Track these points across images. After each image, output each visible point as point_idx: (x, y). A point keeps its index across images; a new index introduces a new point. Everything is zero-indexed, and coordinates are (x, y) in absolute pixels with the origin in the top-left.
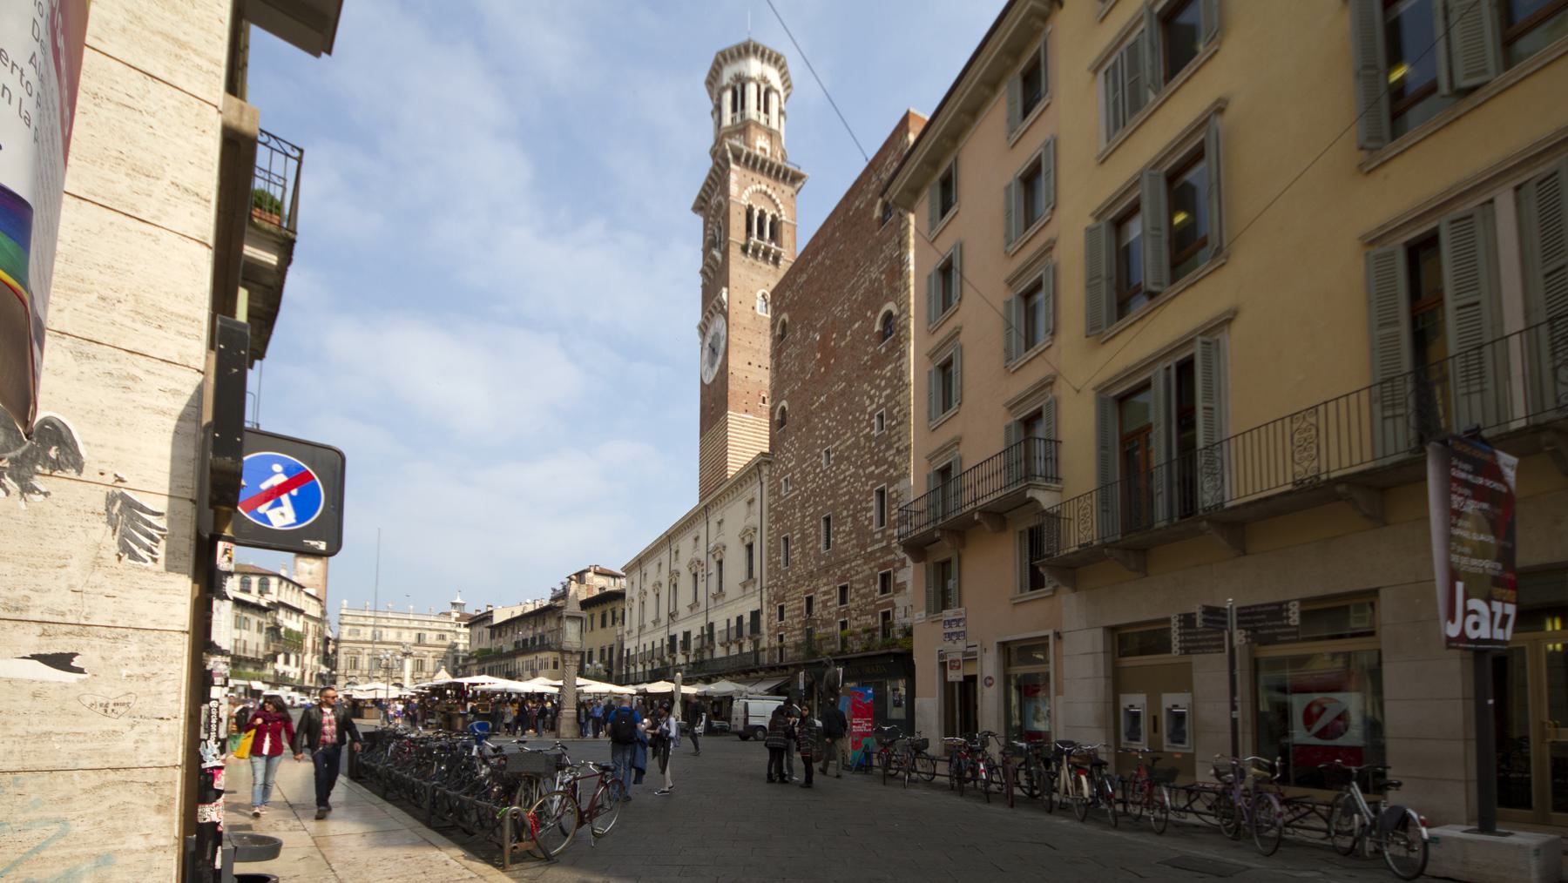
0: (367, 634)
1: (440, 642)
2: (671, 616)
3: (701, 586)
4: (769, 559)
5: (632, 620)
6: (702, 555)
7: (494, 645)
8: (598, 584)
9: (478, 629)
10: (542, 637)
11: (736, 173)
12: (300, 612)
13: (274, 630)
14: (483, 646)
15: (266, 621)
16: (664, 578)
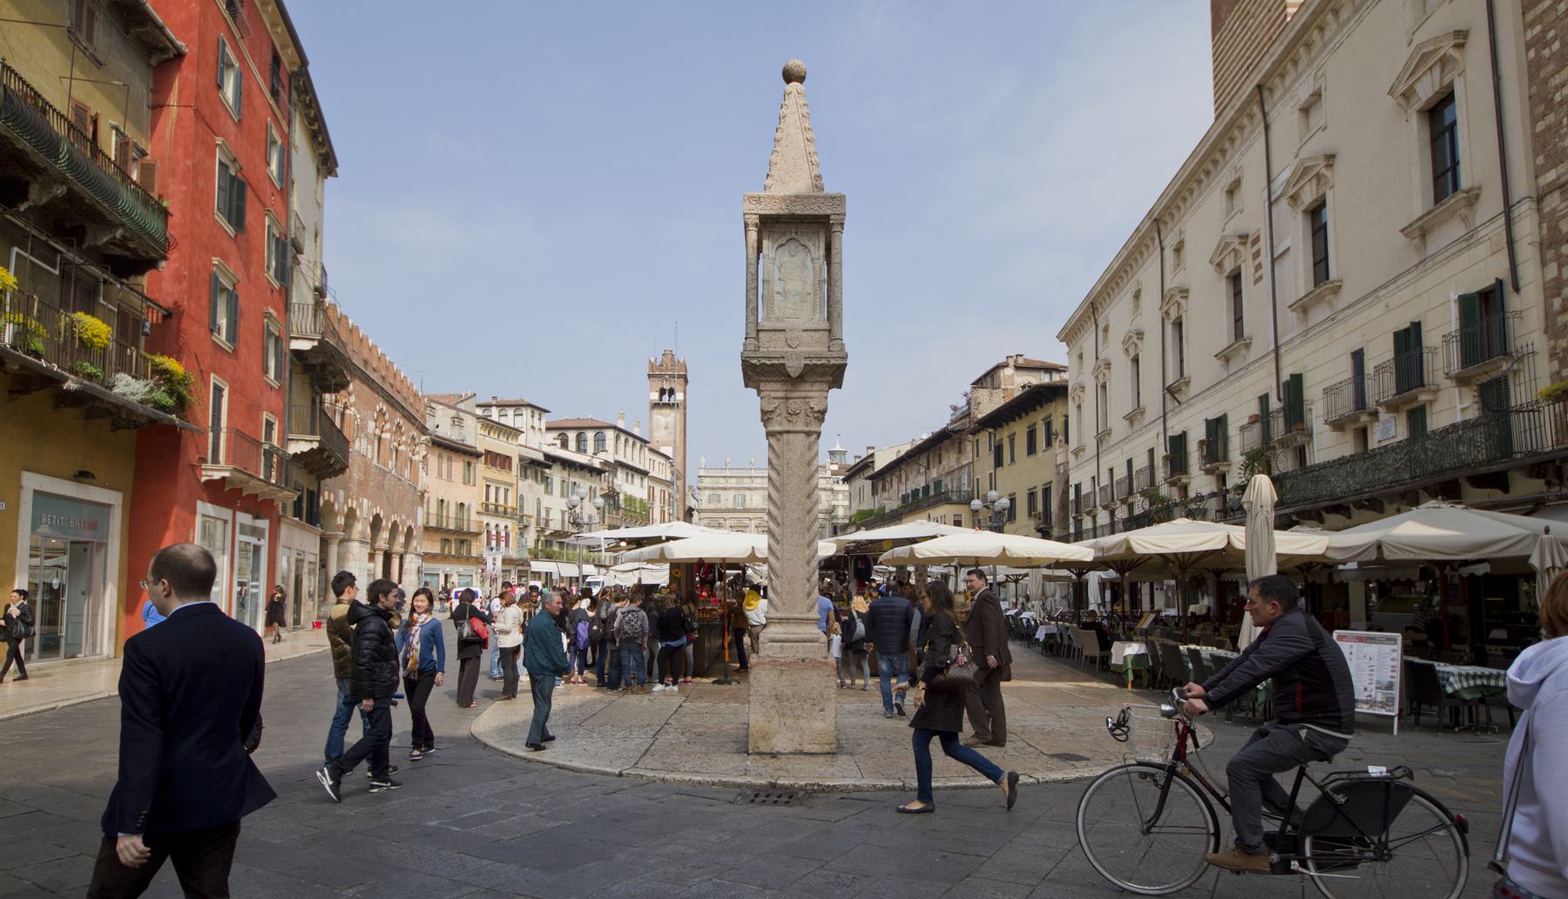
3: (1255, 297)
5: (1083, 428)
6: (1251, 215)
10: (938, 483)
12: (644, 473)
13: (611, 495)
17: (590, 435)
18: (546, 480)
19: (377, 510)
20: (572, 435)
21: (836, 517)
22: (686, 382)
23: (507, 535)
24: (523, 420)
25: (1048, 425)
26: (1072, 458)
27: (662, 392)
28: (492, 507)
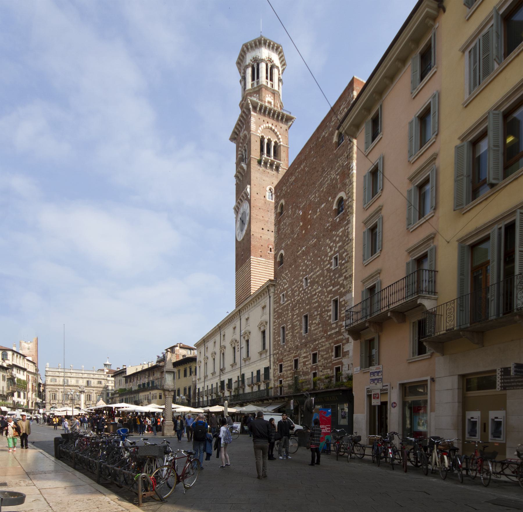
0: (60, 381)
2: (222, 370)
3: (238, 354)
4: (274, 339)
5: (201, 372)
7: (128, 386)
8: (182, 353)
10: (153, 382)
11: (254, 117)
13: (12, 379)
14: (122, 387)
15: (7, 375)
16: (217, 350)
25: (191, 369)
26: (197, 381)
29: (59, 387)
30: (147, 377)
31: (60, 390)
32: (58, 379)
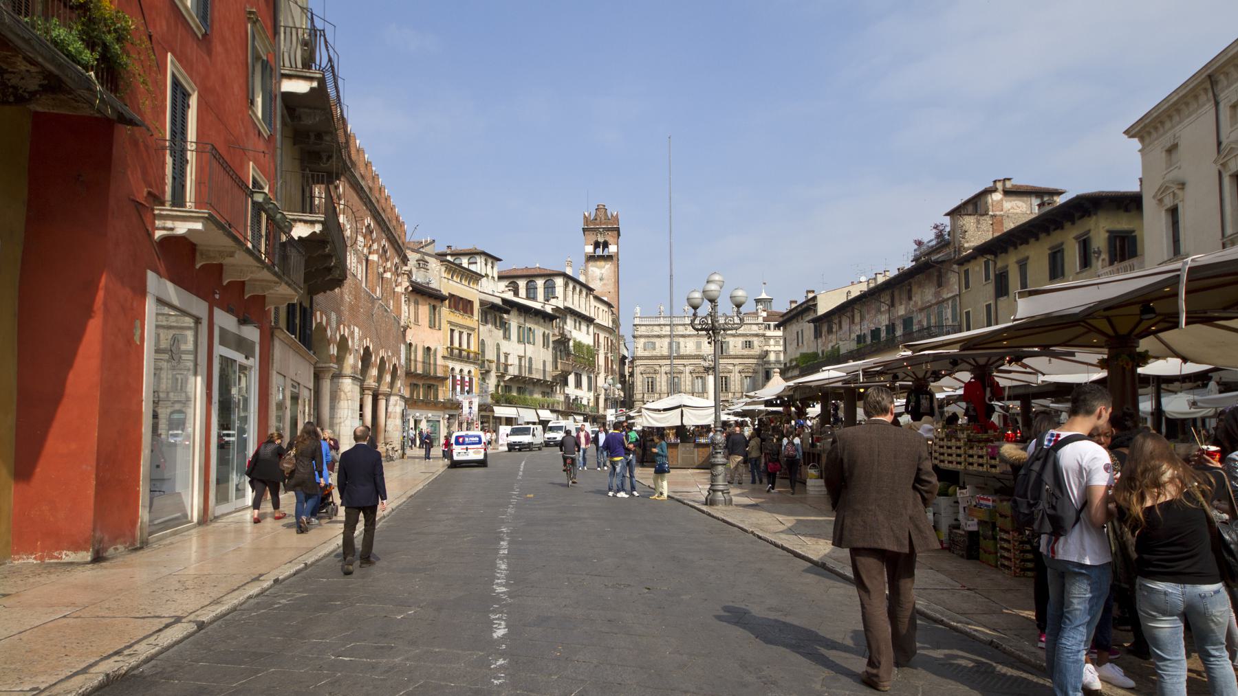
0: (662, 347)
1: (746, 352)
9: (794, 328)
10: (908, 322)
12: (589, 321)
13: (562, 344)
14: (805, 350)
15: (553, 333)
17: (540, 283)
18: (504, 326)
19: (367, 342)
20: (522, 284)
21: (768, 363)
22: (619, 235)
23: (471, 380)
24: (479, 266)
27: (597, 245)
28: (456, 352)
29: (660, 362)
30: (884, 308)
31: (664, 369)
32: (658, 341)
